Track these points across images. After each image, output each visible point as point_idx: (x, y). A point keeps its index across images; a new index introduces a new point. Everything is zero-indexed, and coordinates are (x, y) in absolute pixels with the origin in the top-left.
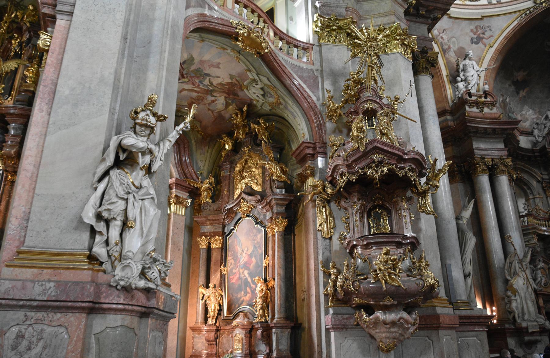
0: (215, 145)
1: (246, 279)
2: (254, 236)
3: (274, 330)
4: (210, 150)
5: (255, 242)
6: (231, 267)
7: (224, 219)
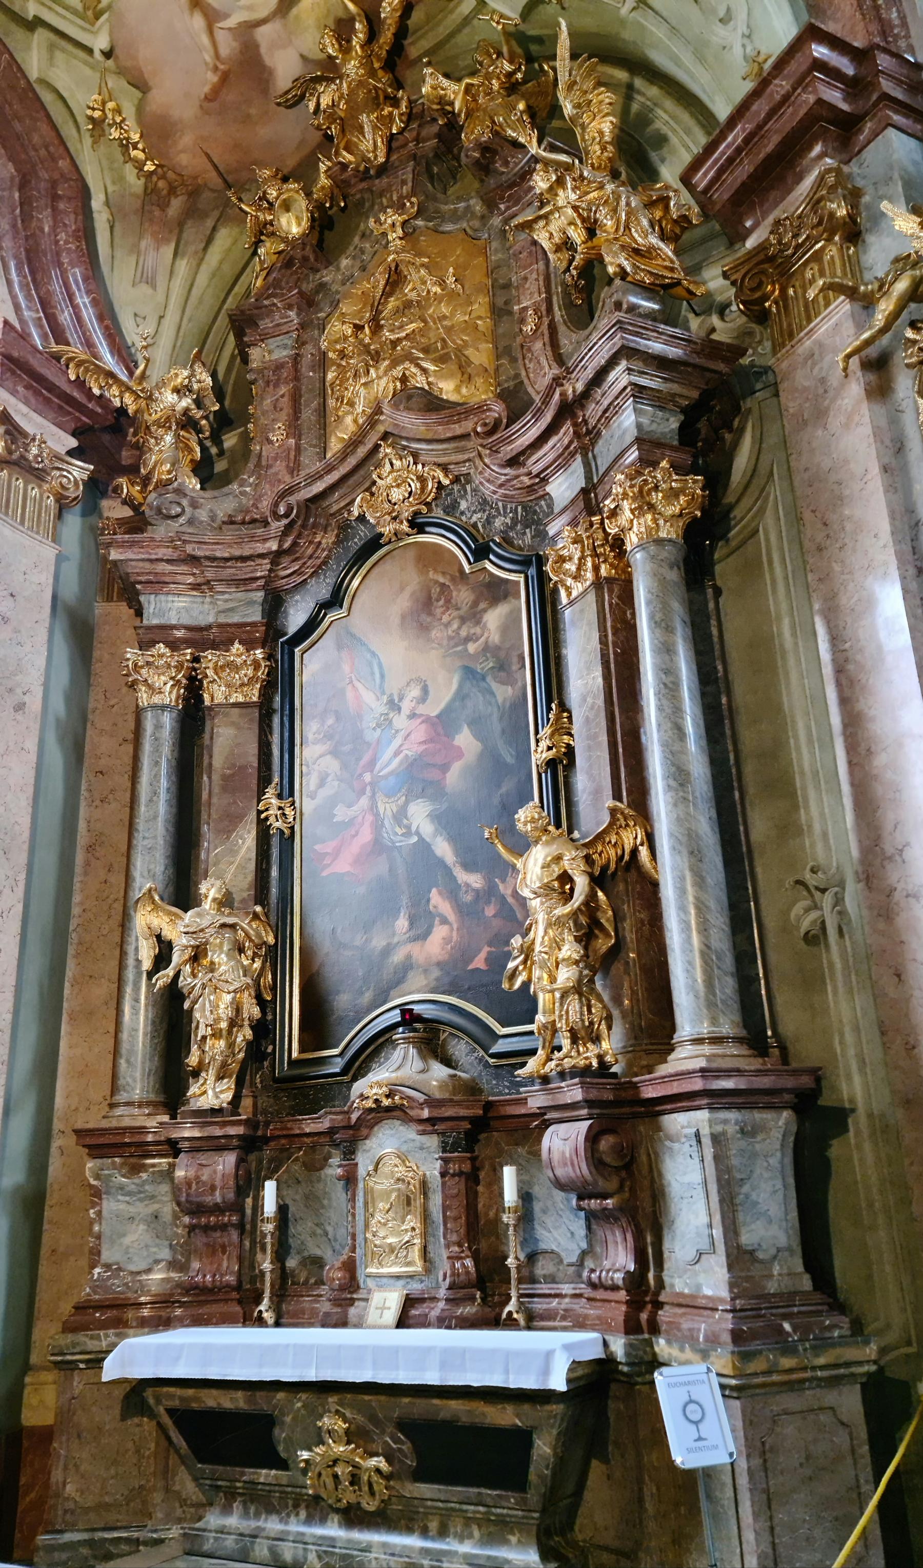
0: (209, 241)
1: (423, 847)
2: (463, 620)
3: (682, 1123)
4: (183, 266)
5: (472, 648)
6: (323, 794)
7: (276, 557)
